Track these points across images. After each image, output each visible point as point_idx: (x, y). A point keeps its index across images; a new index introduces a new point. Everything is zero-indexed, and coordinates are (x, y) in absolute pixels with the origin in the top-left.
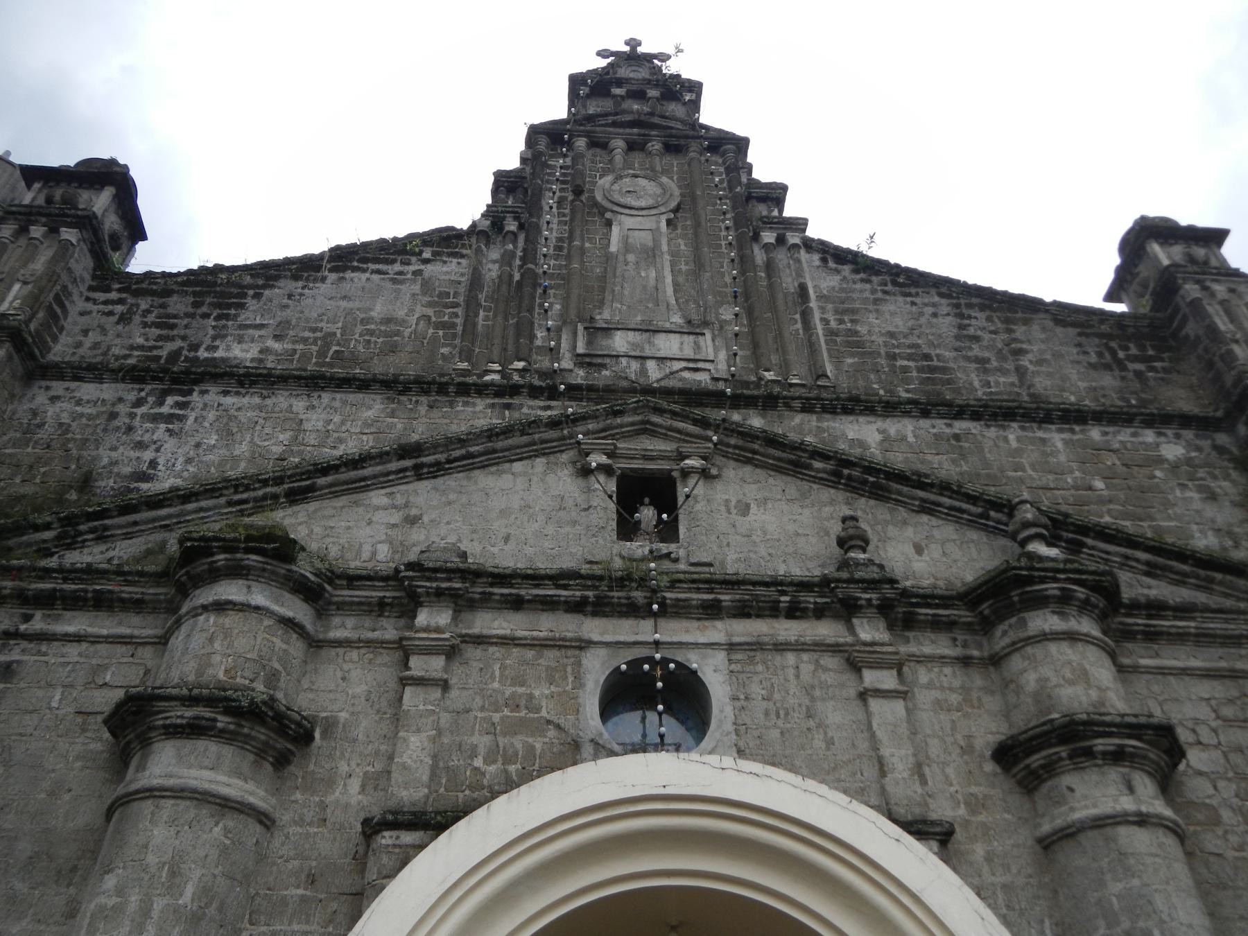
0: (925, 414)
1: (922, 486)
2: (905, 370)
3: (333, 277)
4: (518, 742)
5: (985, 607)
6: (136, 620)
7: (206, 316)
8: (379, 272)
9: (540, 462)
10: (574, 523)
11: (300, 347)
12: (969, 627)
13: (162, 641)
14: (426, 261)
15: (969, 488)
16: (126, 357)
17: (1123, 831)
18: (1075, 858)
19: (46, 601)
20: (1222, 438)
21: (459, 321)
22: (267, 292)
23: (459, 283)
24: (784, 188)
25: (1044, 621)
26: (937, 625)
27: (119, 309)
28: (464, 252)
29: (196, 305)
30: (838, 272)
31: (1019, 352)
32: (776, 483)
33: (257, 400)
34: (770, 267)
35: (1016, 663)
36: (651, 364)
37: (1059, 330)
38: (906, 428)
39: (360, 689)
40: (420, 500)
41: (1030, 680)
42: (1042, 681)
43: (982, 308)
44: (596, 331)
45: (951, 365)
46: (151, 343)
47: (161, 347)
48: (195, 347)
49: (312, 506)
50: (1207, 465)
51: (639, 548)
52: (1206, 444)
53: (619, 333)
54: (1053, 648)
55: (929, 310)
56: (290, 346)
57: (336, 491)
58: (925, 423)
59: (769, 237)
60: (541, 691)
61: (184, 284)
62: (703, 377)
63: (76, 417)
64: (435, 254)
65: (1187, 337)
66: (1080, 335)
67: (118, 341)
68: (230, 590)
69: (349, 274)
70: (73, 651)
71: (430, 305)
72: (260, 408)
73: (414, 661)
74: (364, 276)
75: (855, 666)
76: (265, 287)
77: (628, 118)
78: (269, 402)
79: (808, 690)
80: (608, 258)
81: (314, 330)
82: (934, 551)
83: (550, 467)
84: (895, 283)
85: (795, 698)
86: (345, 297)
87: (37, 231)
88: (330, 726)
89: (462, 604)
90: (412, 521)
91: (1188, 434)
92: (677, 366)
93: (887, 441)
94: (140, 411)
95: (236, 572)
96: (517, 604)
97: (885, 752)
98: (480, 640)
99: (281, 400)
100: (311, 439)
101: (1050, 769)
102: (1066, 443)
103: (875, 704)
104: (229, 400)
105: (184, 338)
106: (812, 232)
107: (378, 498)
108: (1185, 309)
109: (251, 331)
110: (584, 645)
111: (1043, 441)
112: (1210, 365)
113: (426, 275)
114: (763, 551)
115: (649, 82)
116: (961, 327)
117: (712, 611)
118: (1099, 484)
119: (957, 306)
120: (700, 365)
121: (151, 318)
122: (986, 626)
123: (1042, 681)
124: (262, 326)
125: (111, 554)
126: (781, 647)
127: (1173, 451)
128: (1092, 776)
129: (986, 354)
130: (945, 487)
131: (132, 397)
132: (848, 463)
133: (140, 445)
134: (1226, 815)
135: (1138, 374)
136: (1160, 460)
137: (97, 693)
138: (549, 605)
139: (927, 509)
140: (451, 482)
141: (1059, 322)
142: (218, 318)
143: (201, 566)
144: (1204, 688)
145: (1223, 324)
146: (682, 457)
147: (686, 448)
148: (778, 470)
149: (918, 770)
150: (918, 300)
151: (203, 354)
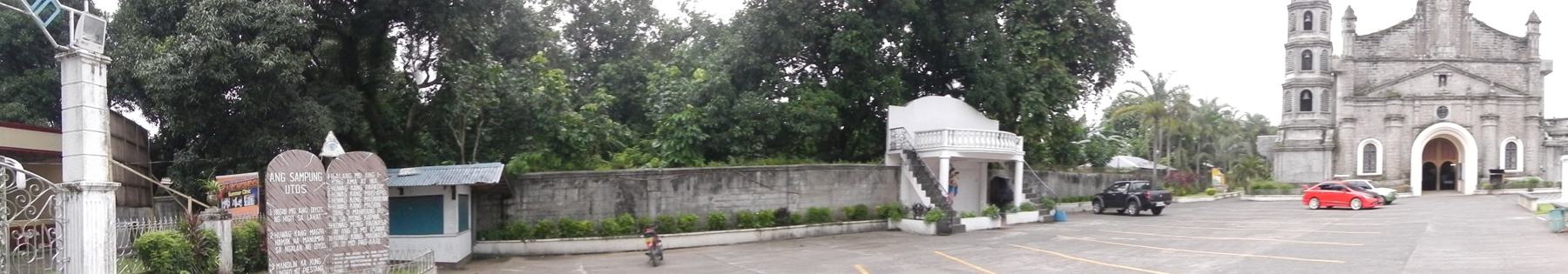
20: (1526, 66)
25: (1489, 101)
32: (1462, 76)
34: (1466, 25)
35: (1485, 106)
38: (1480, 65)
43: (1500, 36)
44: (1437, 47)
51: (1441, 89)
59: (1466, 18)
68: (1394, 102)
80: (1439, 26)
88: (1406, 116)
89: (1420, 100)
93: (1478, 68)
99: (1390, 64)
106: (1474, 16)
107: (1407, 82)
145: (1533, 45)
149: (1471, 119)
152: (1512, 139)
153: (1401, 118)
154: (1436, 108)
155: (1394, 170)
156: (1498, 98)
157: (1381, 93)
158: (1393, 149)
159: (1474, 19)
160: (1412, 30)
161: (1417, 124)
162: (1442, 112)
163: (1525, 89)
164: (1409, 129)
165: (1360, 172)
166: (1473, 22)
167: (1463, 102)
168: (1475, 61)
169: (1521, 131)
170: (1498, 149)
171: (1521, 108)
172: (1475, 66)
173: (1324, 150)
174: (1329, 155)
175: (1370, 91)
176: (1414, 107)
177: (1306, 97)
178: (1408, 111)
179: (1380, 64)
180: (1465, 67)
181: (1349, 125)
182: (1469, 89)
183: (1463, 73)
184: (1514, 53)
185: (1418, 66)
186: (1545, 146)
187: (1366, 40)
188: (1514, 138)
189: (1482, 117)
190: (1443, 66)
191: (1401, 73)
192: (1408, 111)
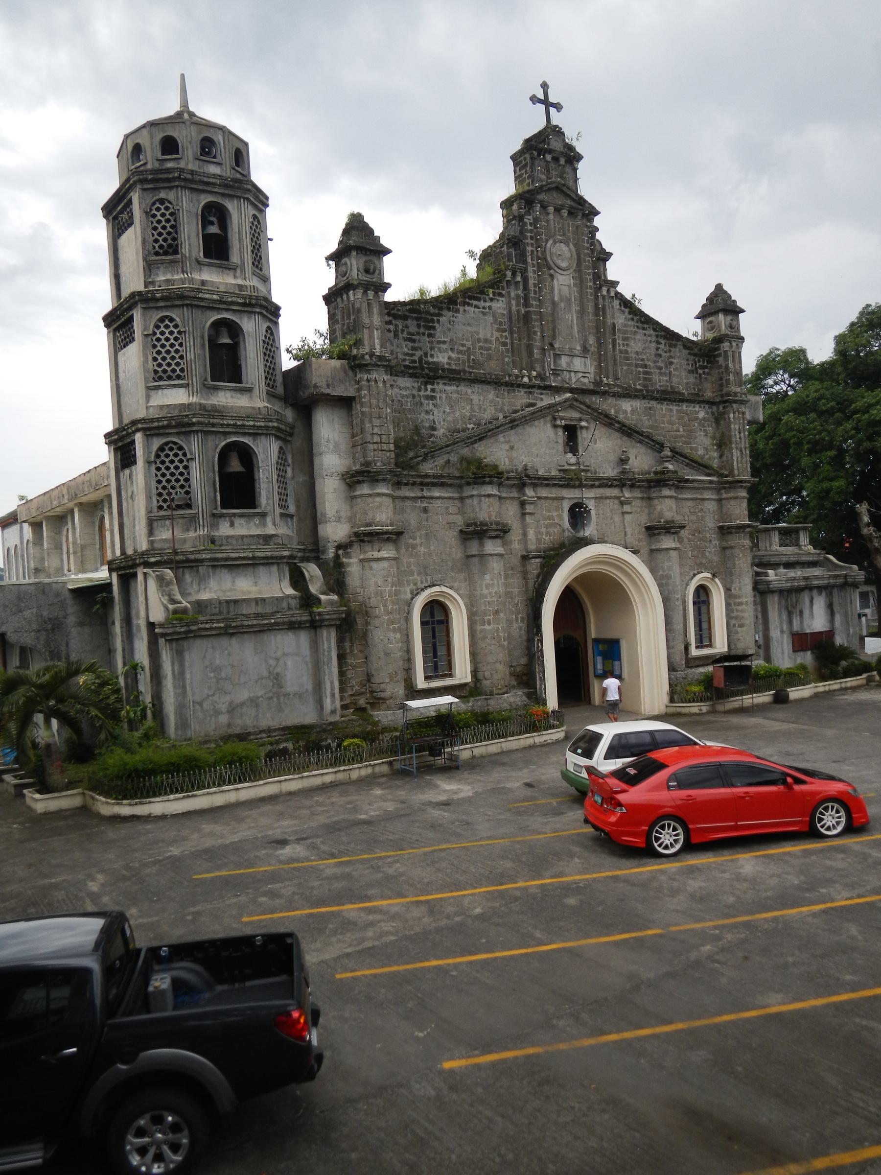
0: (644, 398)
1: (642, 435)
2: (639, 373)
3: (461, 308)
4: (551, 530)
5: (652, 484)
6: (450, 490)
7: (424, 334)
8: (477, 307)
9: (542, 420)
10: (553, 448)
11: (460, 356)
12: (645, 487)
13: (462, 499)
14: (492, 300)
15: (654, 438)
16: (405, 360)
17: (671, 551)
18: (660, 556)
19: (427, 484)
20: (715, 408)
21: (508, 341)
22: (441, 319)
23: (504, 315)
24: (610, 255)
25: (666, 492)
26: (639, 487)
27: (392, 327)
28: (503, 292)
29: (419, 326)
30: (624, 312)
31: (671, 363)
33: (454, 388)
35: (656, 502)
36: (573, 374)
37: (684, 351)
38: (637, 404)
39: (511, 513)
40: (512, 439)
41: (659, 508)
42: (662, 509)
43: (665, 338)
44: (557, 356)
45: (652, 371)
46: (411, 352)
47: (414, 355)
48: (426, 355)
49: (484, 442)
50: (709, 421)
52: (710, 411)
53: (563, 357)
54: (666, 500)
55: (649, 339)
56: (457, 356)
57: (491, 437)
58: (643, 401)
59: (604, 291)
60: (555, 514)
61: (410, 311)
62: (586, 380)
63: (403, 396)
64: (494, 294)
65: (718, 362)
66: (689, 354)
67: (398, 350)
69: (467, 308)
70: (439, 502)
71: (498, 330)
72: (458, 392)
73: (527, 506)
74: (473, 309)
75: (622, 503)
76: (440, 315)
77: (554, 185)
78: (459, 389)
79: (611, 511)
80: (554, 303)
81: (463, 345)
82: (639, 459)
83: (545, 422)
84: (642, 322)
85: (609, 514)
86: (469, 324)
87: (371, 294)
89: (535, 486)
90: (512, 448)
91: (707, 406)
92: (581, 375)
93: (634, 411)
94: (422, 393)
95: (490, 483)
96: (547, 485)
97: (627, 529)
98: (539, 498)
99: (464, 389)
100: (476, 408)
101: (659, 534)
102: (677, 411)
103: (626, 516)
104: (447, 388)
105: (421, 349)
106: (619, 289)
107: (501, 438)
108: (721, 351)
109: (442, 346)
110: (563, 498)
111: (671, 410)
112: (721, 379)
113: (493, 308)
114: (600, 459)
115: (562, 153)
116: (657, 349)
117: (592, 486)
118: (681, 430)
119: (657, 336)
120: (587, 375)
121: (405, 335)
122: (650, 487)
123: (662, 509)
124: (444, 342)
125: (436, 463)
126: (607, 498)
127: (701, 415)
128: (668, 537)
129: (662, 365)
130: (648, 437)
131: (416, 385)
132: (625, 426)
133: (427, 412)
134: (685, 540)
135: (700, 375)
136: (697, 418)
137: (450, 516)
138: (555, 485)
139: (640, 442)
140: (519, 430)
141: (685, 347)
142: (430, 335)
143: (479, 481)
144: (690, 503)
146: (580, 420)
147: (585, 417)
148: (604, 424)
150: (647, 332)
151: (430, 360)
152: (703, 577)
153: (502, 532)
154: (566, 506)
155: (500, 667)
156: (680, 484)
157: (448, 461)
158: (497, 612)
159: (619, 296)
160: (499, 306)
161: (532, 546)
162: (578, 514)
163: (715, 464)
164: (515, 560)
165: (421, 683)
166: (616, 303)
167: (615, 492)
168: (628, 394)
169: (716, 559)
170: (684, 603)
171: (711, 506)
172: (627, 406)
173: (315, 625)
174: (329, 639)
175: (425, 459)
176: (523, 504)
177: (235, 466)
178: (510, 513)
179: (440, 386)
180: (609, 405)
181: (387, 552)
182: (623, 461)
183: (609, 421)
184: (692, 379)
185: (521, 398)
186: (762, 590)
187: (405, 318)
188: (709, 575)
189: (648, 528)
190: (569, 405)
191: (487, 416)
192: (510, 513)
